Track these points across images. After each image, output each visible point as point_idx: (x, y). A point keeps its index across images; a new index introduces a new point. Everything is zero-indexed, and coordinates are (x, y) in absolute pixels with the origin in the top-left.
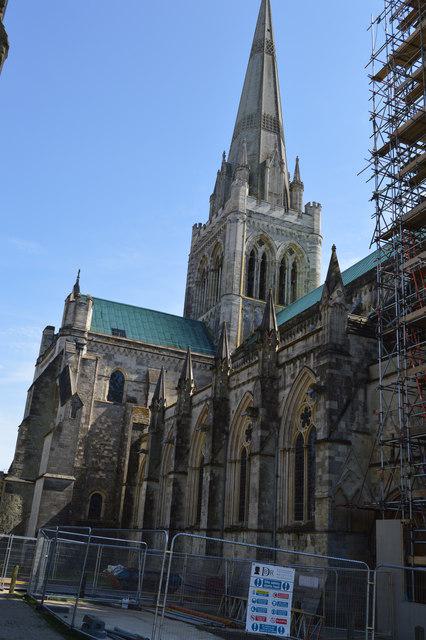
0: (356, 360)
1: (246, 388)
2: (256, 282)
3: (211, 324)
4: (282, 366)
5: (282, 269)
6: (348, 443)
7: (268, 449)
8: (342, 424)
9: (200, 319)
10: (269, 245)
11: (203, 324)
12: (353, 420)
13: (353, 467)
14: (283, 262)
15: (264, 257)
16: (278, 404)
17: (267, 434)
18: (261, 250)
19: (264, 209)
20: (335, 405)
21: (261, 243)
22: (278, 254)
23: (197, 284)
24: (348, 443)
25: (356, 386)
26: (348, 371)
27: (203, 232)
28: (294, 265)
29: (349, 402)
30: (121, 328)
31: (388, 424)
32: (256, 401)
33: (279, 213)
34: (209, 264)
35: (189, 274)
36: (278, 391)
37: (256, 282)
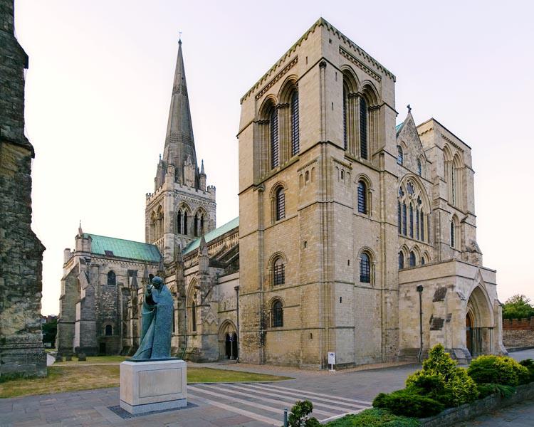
0: (212, 276)
1: (173, 283)
2: (182, 226)
3: (160, 246)
4: (184, 276)
5: (196, 219)
6: (209, 306)
7: (182, 307)
8: (207, 299)
9: (154, 244)
10: (188, 208)
11: (156, 246)
12: (211, 298)
13: (211, 313)
14: (196, 216)
15: (186, 213)
16: (184, 290)
17: (180, 302)
18: (184, 211)
19: (185, 189)
20: (203, 293)
21: (183, 206)
22: (193, 213)
23: (151, 225)
24: (209, 306)
25: (213, 286)
26: (208, 280)
27: (152, 199)
28: (202, 217)
29: (209, 291)
30: (110, 250)
32: (176, 291)
33: (193, 191)
34: (156, 216)
35: (147, 219)
36: (184, 286)
37: (182, 226)
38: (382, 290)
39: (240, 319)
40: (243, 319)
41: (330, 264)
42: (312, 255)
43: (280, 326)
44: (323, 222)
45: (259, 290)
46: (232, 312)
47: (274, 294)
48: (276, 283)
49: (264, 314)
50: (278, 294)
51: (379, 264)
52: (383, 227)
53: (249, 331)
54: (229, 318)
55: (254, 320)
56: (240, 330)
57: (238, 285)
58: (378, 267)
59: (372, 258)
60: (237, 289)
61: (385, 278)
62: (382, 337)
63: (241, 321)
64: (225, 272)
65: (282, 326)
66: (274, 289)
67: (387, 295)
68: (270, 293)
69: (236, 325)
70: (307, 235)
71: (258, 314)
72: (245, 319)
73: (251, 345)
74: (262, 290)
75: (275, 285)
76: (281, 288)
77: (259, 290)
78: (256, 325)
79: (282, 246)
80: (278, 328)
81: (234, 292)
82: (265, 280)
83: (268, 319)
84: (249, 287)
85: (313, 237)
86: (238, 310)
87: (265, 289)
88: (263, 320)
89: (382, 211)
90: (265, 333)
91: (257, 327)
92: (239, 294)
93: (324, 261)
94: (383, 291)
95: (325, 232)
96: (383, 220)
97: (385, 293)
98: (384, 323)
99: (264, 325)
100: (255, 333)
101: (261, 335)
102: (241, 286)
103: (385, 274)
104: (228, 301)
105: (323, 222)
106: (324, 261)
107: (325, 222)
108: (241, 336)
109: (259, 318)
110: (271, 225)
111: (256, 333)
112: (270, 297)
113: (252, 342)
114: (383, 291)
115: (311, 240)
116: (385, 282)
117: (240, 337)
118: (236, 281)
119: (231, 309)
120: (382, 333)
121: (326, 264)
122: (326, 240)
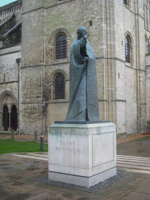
31: (3, 71)
38: (137, 70)
39: (20, 90)
40: (23, 91)
41: (112, 43)
42: (97, 33)
43: (61, 98)
44: (106, 5)
45: (42, 63)
46: (12, 84)
47: (57, 67)
48: (58, 57)
49: (45, 86)
50: (60, 68)
51: (135, 47)
52: (136, 17)
53: (30, 103)
54: (9, 89)
55: (36, 91)
56: (21, 100)
57: (20, 57)
58: (134, 50)
59: (131, 42)
60: (18, 61)
61: (139, 60)
62: (137, 111)
63: (21, 93)
64: (4, 44)
65: (64, 98)
66: (56, 63)
67: (141, 75)
68: (52, 67)
69: (17, 97)
70: (92, 15)
71: (40, 86)
72: (26, 90)
73: (32, 116)
74: (45, 64)
75: (56, 59)
76: (63, 61)
77: (42, 63)
78: (39, 97)
79: (64, 24)
80: (60, 100)
81: (14, 62)
82: (47, 54)
83: (50, 91)
84: (31, 60)
85: (97, 17)
86: (18, 82)
87: (47, 62)
88: (44, 92)
89: (136, 5)
90: (47, 105)
91: (39, 99)
92: (20, 67)
93: (107, 40)
94: (138, 71)
95: (108, 14)
96: (136, 12)
97: (139, 73)
98: (139, 98)
99: (46, 97)
100: (37, 105)
101: (43, 107)
102: (23, 59)
103: (139, 57)
104: (8, 73)
105: (106, 5)
106: (107, 40)
107: (108, 6)
108: (21, 108)
109: (41, 89)
110: (54, 5)
111: (38, 105)
112: (52, 70)
113: (33, 113)
114: (138, 71)
115: (96, 20)
116: (139, 64)
117: (21, 109)
118: (17, 53)
119: (12, 80)
120: (138, 107)
121: (109, 42)
122: (108, 22)
